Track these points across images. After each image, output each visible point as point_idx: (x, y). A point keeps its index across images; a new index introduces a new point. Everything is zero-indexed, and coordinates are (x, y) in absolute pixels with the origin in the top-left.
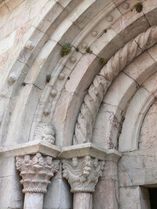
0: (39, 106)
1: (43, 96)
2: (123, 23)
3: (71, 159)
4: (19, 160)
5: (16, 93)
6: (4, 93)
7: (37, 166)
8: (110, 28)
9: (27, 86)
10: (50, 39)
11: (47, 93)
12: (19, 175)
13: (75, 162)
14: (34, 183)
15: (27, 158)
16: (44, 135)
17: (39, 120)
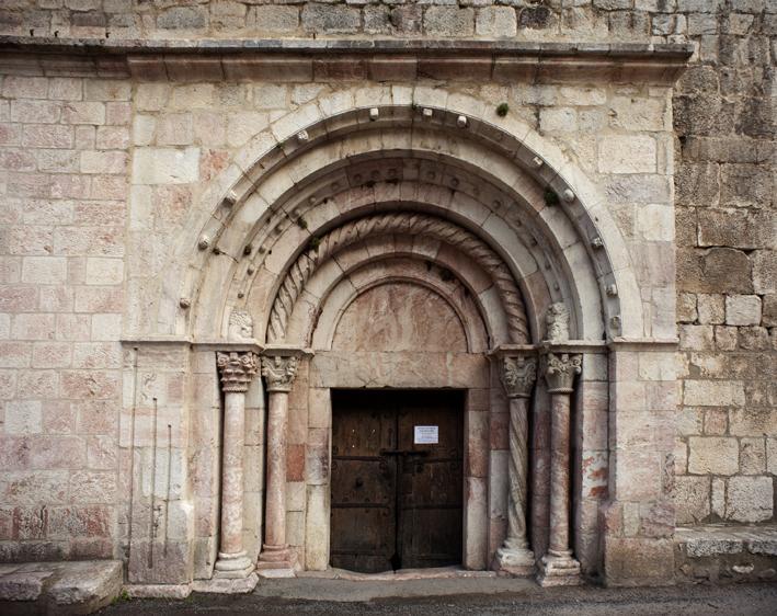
0: (233, 285)
1: (239, 271)
2: (350, 200)
3: (272, 358)
4: (221, 356)
5: (207, 263)
6: (192, 262)
7: (248, 366)
8: (332, 199)
9: (221, 256)
10: (258, 193)
11: (245, 271)
12: (220, 371)
13: (278, 360)
14: (242, 383)
15: (235, 356)
16: (244, 326)
17: (234, 304)
